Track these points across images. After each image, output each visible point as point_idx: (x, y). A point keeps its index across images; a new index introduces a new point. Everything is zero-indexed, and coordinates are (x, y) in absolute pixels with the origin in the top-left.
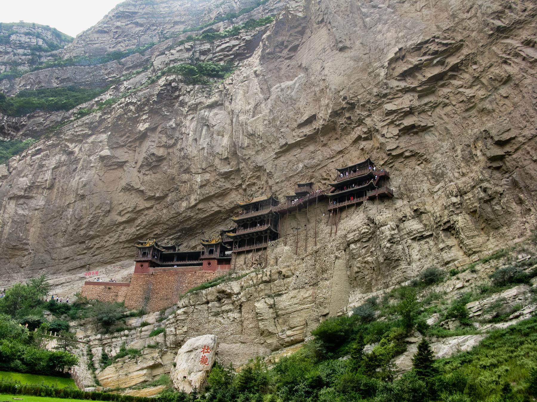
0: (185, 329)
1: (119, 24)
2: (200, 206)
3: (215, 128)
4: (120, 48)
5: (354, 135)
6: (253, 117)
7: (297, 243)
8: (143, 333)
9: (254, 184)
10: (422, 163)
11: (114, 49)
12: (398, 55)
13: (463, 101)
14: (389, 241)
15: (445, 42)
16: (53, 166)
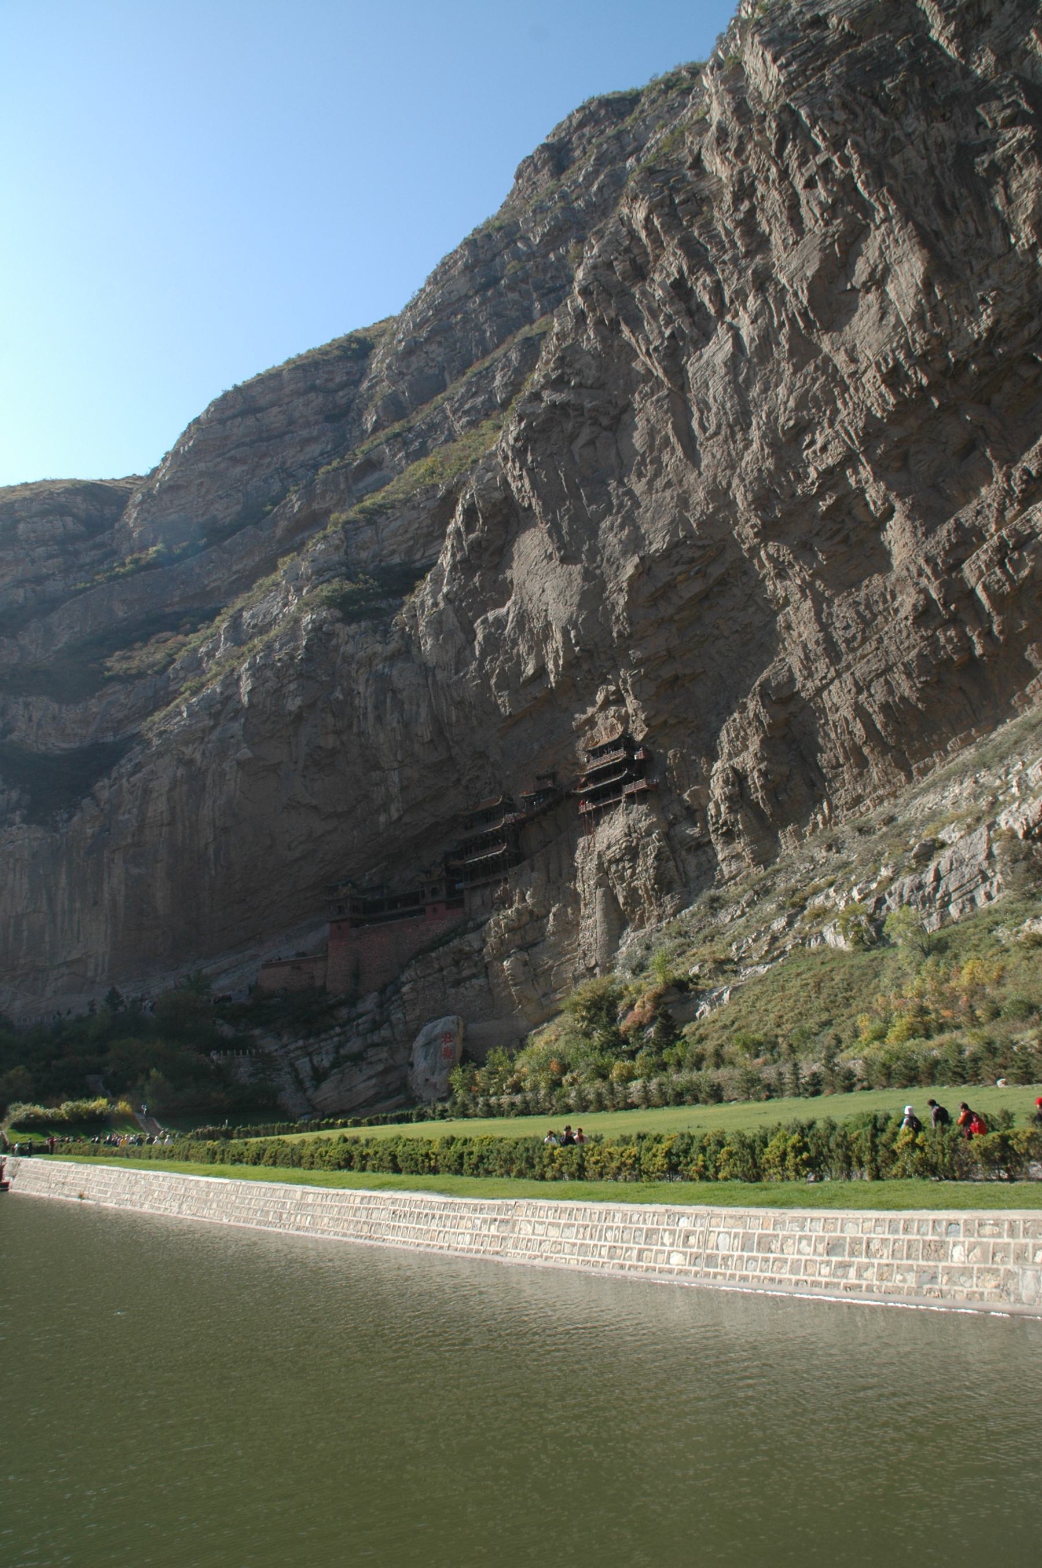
0: (418, 1012)
1: (202, 466)
2: (406, 819)
3: (405, 693)
4: (216, 513)
5: (600, 697)
6: (457, 672)
7: (549, 863)
8: (361, 1028)
9: (478, 777)
10: (693, 732)
11: (205, 518)
12: (641, 570)
13: (737, 631)
14: (655, 858)
15: (700, 543)
16: (166, 789)
